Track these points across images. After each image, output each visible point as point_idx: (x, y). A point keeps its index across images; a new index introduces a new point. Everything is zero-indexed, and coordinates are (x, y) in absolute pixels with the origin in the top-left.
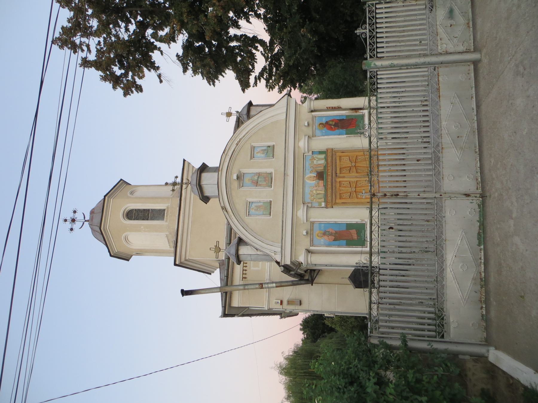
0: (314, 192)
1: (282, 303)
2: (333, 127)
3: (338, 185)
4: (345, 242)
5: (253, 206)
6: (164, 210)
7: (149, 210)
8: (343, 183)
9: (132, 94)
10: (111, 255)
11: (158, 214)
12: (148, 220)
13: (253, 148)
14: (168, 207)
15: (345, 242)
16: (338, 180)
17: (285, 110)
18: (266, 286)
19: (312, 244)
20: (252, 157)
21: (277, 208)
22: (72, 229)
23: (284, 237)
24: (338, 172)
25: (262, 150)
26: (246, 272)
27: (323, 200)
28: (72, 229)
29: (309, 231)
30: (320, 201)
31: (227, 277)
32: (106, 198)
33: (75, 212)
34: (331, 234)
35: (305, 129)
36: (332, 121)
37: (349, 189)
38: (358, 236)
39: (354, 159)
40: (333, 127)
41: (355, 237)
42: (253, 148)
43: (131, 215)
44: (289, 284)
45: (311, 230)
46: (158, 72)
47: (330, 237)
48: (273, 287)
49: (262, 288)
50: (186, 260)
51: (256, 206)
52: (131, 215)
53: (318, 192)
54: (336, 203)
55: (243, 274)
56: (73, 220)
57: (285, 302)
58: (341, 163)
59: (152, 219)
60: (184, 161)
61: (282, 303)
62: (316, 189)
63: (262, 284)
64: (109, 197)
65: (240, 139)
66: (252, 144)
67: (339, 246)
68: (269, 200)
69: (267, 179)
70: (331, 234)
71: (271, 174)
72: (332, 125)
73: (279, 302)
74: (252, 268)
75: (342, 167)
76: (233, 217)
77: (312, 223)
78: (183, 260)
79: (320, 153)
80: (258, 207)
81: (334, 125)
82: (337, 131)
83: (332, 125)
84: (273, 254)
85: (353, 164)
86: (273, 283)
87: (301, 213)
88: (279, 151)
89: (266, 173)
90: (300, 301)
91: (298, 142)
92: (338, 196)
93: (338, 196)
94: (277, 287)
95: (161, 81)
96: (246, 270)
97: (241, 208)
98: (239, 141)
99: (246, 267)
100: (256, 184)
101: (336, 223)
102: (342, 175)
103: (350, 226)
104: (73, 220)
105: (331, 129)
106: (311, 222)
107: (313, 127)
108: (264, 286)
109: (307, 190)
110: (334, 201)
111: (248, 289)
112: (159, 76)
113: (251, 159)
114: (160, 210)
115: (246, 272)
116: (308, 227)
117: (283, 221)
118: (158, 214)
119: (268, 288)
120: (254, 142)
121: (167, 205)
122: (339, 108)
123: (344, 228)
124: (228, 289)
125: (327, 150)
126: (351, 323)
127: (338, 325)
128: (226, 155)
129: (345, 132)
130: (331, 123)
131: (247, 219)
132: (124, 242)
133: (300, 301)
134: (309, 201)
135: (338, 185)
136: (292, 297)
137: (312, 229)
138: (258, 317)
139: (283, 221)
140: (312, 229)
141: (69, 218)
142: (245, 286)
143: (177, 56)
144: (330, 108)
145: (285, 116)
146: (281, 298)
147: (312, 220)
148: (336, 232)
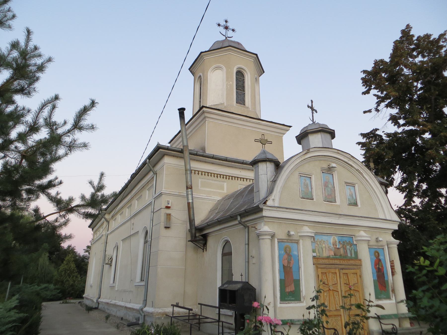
0: (324, 245)
1: (168, 207)
2: (378, 266)
3: (333, 271)
4: (283, 278)
5: (308, 181)
6: (244, 105)
7: (244, 91)
8: (335, 276)
9: (362, 85)
10: (202, 53)
11: (241, 100)
12: (236, 89)
13: (353, 185)
14: (248, 108)
15: (283, 278)
16: (337, 271)
17: (388, 218)
18: (190, 193)
19: (280, 241)
20: (347, 184)
21: (308, 205)
22: (219, 25)
23: (288, 210)
24: (344, 271)
25: (352, 194)
26: (197, 174)
27: (318, 255)
28: (219, 25)
29: (291, 238)
30: (317, 251)
31: (196, 155)
32: (255, 56)
33: (233, 30)
34: (289, 263)
35: (374, 238)
36: (382, 266)
37: (330, 284)
38: (289, 293)
39: (356, 289)
40: (378, 266)
41: (288, 290)
42: (353, 185)
43: (240, 75)
44: (192, 216)
45: (291, 240)
46: (373, 110)
47: (286, 261)
48: (188, 200)
49: (187, 188)
50: (205, 117)
51: (307, 184)
52: (240, 75)
53: (324, 249)
54: (317, 268)
55: (195, 171)
56: (226, 28)
57: (168, 211)
58: (351, 275)
59: (237, 92)
60: (290, 127)
61: (168, 207)
62: (327, 247)
63: (191, 188)
64: (255, 58)
65: (361, 174)
66: (357, 185)
67: (280, 271)
68: (314, 197)
69: (330, 199)
70: (289, 263)
71: (335, 201)
72: (379, 265)
73: (169, 205)
74: (200, 180)
75: (349, 275)
76: (301, 160)
77: (297, 242)
78: (206, 115)
79: (356, 253)
80: (306, 186)
81: (379, 268)
82: (375, 270)
83: (379, 265)
84: (273, 198)
85: (331, 288)
86: (193, 199)
87: (307, 230)
88: (353, 211)
89: (335, 197)
90: (169, 227)
91: (364, 231)
92: (324, 271)
93: (324, 271)
94: (189, 203)
95: (365, 112)
96: (198, 174)
97: (306, 169)
98: (360, 172)
99: (202, 174)
100: (326, 185)
101: (299, 268)
102: (342, 275)
103: (297, 283)
104: (226, 28)
105: (376, 265)
106: (298, 240)
107: (375, 246)
108: (189, 190)
109: (325, 238)
110: (319, 266)
111: (186, 174)
112: (370, 111)
113: (346, 183)
114: (244, 101)
115: (197, 174)
116: (295, 238)
117: (302, 210)
118: (241, 100)
119: (187, 195)
120: (358, 186)
121: (250, 107)
122: (393, 274)
123: (295, 277)
124: (186, 154)
125: (360, 260)
126: (67, 281)
127: (66, 267)
128: (350, 159)
129: (375, 279)
130: (380, 264)
131: (296, 174)
132: (214, 66)
133: (169, 227)
134: (316, 240)
135: (333, 271)
136: (173, 219)
137: (293, 241)
138: (123, 185)
139: (302, 210)
140: (293, 241)
141: (228, 24)
142: (189, 171)
143: (377, 130)
144: (393, 263)
145: (382, 218)
146: (171, 208)
147: (301, 241)
148: (291, 268)
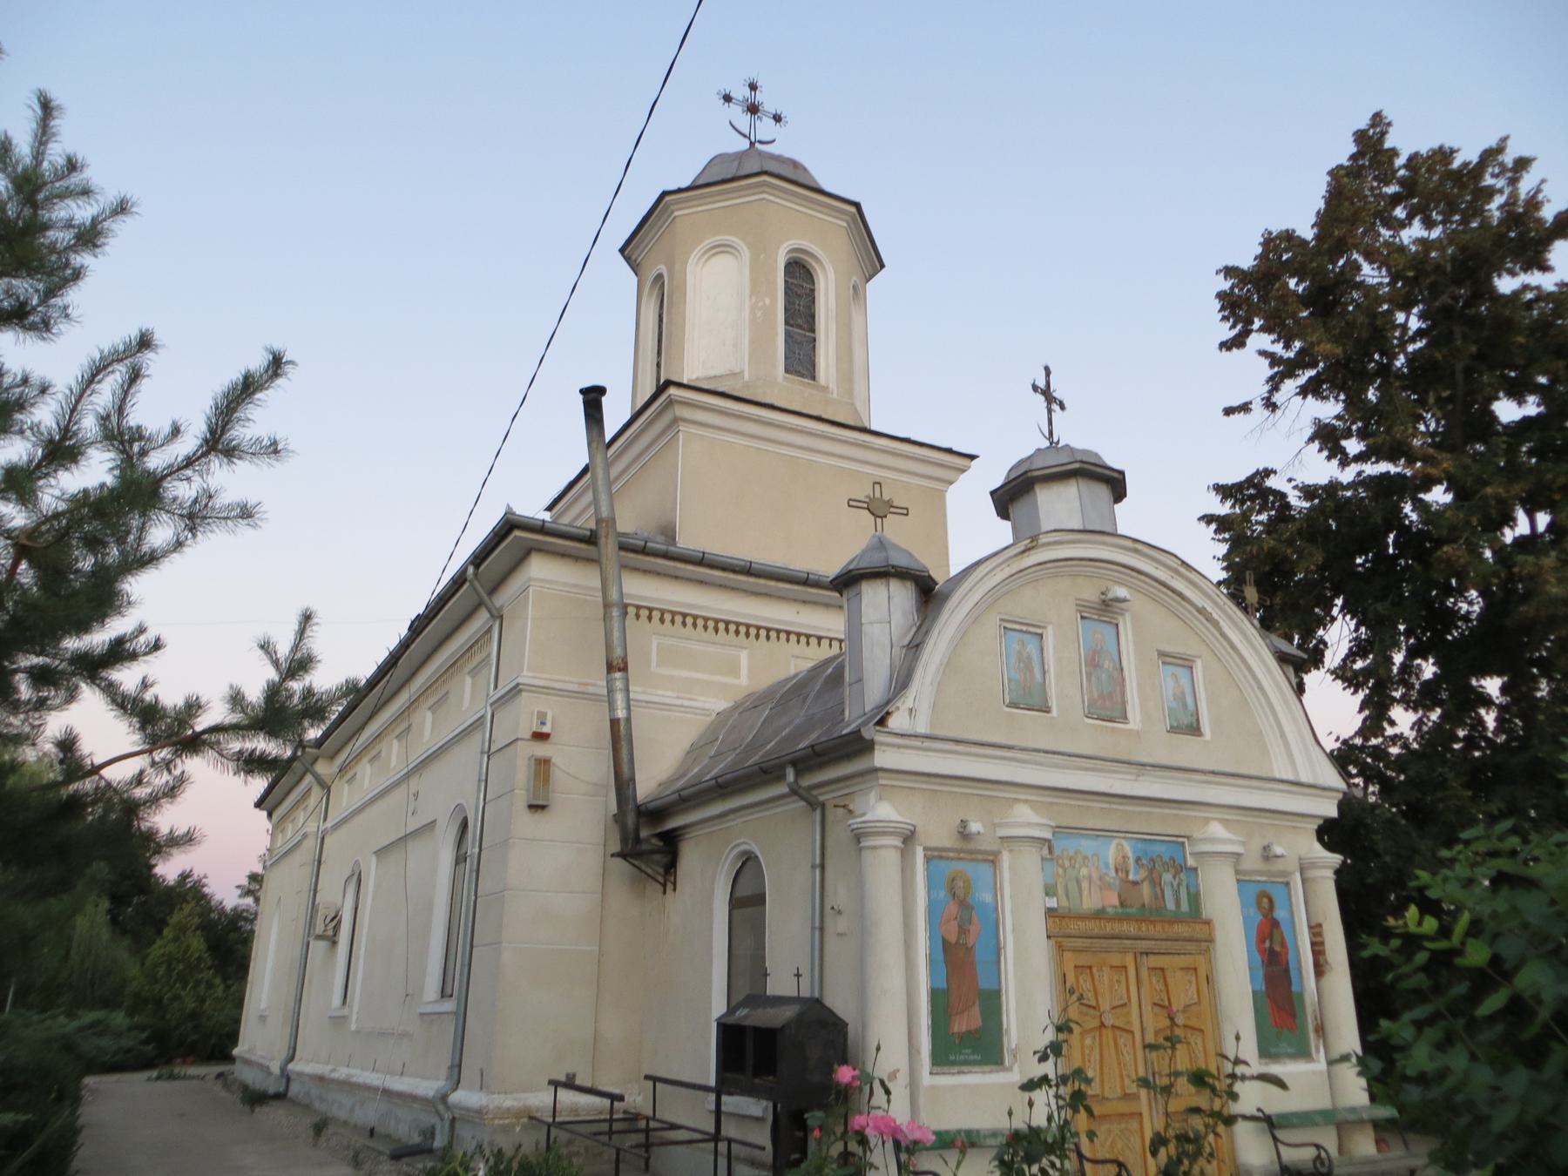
0: (1084, 871)
1: (540, 737)
2: (1267, 944)
5: (1032, 647)
6: (813, 378)
7: (813, 331)
10: (665, 194)
11: (801, 360)
12: (787, 323)
13: (1187, 663)
14: (825, 389)
16: (1129, 961)
17: (1304, 779)
18: (619, 684)
19: (934, 855)
21: (1030, 729)
22: (727, 98)
23: (960, 748)
24: (1154, 961)
25: (1183, 694)
27: (1065, 903)
28: (727, 98)
29: (971, 846)
30: (1060, 891)
31: (644, 551)
32: (853, 209)
33: (777, 118)
34: (963, 931)
35: (1257, 845)
36: (1283, 945)
37: (1105, 1005)
39: (1194, 1022)
40: (1267, 944)
41: (960, 1025)
42: (1187, 663)
43: (799, 273)
44: (625, 769)
45: (971, 852)
46: (1257, 406)
47: (954, 926)
48: (612, 708)
49: (610, 668)
50: (676, 420)
51: (1029, 658)
52: (799, 273)
53: (1085, 885)
54: (1061, 948)
55: (638, 607)
56: (753, 109)
57: (541, 750)
58: (1179, 974)
59: (788, 335)
60: (972, 457)
61: (540, 737)
62: (1095, 876)
64: (853, 217)
65: (1216, 624)
67: (931, 962)
70: (963, 931)
71: (1124, 717)
73: (546, 729)
75: (1169, 974)
77: (993, 860)
79: (1195, 899)
80: (1026, 663)
82: (1258, 958)
84: (909, 703)
85: (1109, 1020)
86: (628, 708)
87: (1027, 819)
88: (1186, 751)
89: (1124, 703)
90: (543, 807)
92: (1084, 959)
94: (614, 723)
95: (1229, 411)
96: (650, 618)
97: (1029, 603)
98: (1209, 618)
99: (662, 620)
100: (1093, 663)
101: (998, 950)
102: (1144, 973)
103: (992, 1002)
104: (753, 109)
106: (997, 854)
108: (618, 675)
109: (1088, 846)
110: (1069, 943)
111: (607, 617)
112: (1245, 408)
113: (1162, 654)
114: (813, 365)
116: (984, 845)
117: (1010, 748)
118: (801, 360)
119: (610, 691)
121: (833, 386)
122: (1320, 970)
123: (984, 983)
124: (609, 547)
125: (1208, 923)
126: (176, 998)
127: (171, 947)
128: (1177, 571)
130: (1276, 937)
131: (991, 625)
132: (708, 242)
133: (543, 807)
134: (1057, 852)
135: (1115, 959)
136: (558, 777)
137: (975, 856)
138: (382, 656)
139: (1010, 748)
140: (975, 856)
141: (760, 97)
142: (616, 610)
143: (1268, 473)
144: (1320, 934)
145: (1284, 777)
147: (1006, 858)
148: (969, 950)
